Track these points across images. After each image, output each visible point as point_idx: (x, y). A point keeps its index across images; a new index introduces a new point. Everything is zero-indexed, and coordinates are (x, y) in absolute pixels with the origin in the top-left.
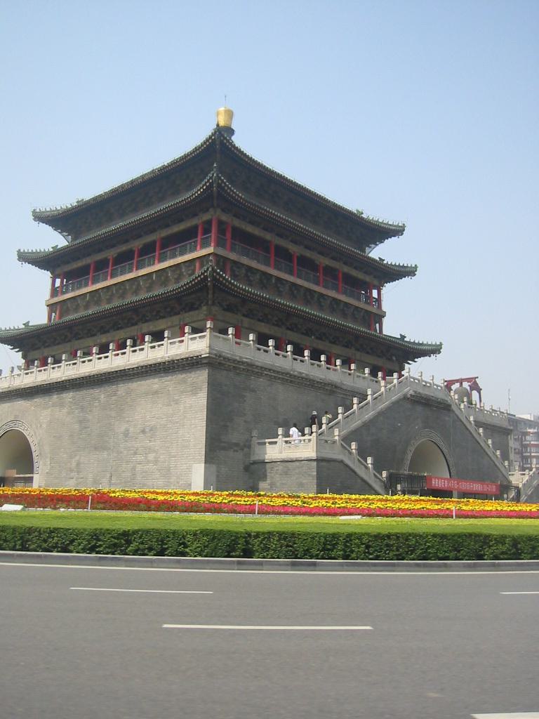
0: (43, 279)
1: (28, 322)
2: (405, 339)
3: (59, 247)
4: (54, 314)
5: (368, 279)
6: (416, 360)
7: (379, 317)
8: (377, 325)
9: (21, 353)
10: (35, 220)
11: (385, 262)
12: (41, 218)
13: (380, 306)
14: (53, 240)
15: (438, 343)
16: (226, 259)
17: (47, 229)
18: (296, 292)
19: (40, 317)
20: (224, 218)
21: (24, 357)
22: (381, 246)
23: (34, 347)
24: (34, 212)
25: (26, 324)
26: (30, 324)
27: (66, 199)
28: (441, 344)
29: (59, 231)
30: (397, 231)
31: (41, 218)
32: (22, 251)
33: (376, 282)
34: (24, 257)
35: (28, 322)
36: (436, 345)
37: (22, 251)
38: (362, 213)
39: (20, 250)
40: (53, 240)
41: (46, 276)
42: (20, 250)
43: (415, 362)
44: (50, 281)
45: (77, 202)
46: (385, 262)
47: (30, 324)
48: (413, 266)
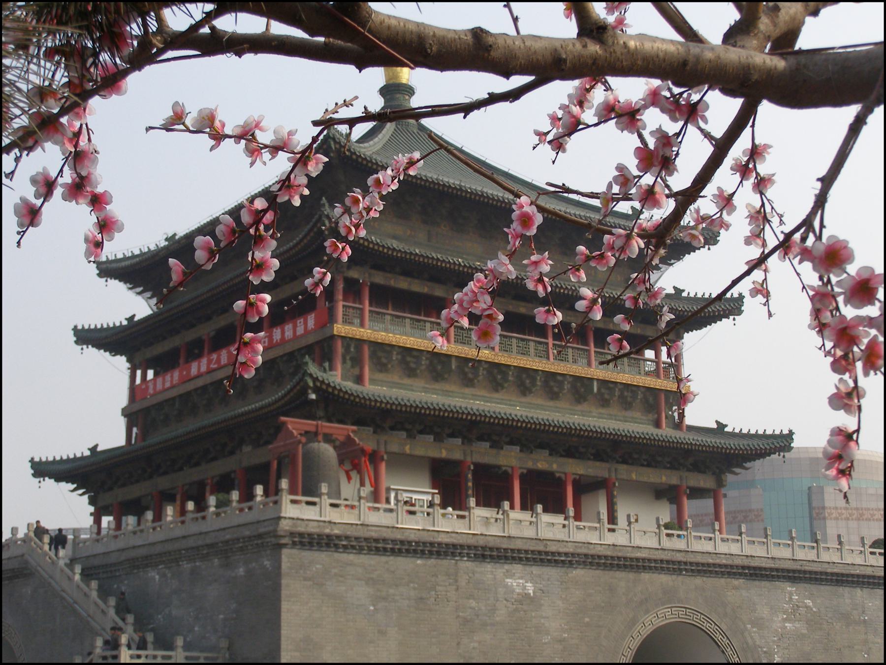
0: (117, 368)
1: (97, 446)
2: (726, 430)
3: (136, 319)
4: (135, 430)
9: (86, 496)
11: (684, 294)
14: (129, 305)
15: (786, 432)
16: (360, 342)
17: (117, 287)
18: (499, 377)
19: (113, 435)
21: (92, 502)
25: (93, 450)
26: (99, 449)
28: (791, 433)
29: (140, 289)
32: (80, 327)
34: (87, 337)
35: (97, 446)
36: (781, 436)
37: (80, 327)
39: (76, 327)
40: (129, 305)
41: (121, 362)
42: (76, 327)
43: (747, 469)
45: (166, 239)
46: (684, 294)
47: (99, 449)
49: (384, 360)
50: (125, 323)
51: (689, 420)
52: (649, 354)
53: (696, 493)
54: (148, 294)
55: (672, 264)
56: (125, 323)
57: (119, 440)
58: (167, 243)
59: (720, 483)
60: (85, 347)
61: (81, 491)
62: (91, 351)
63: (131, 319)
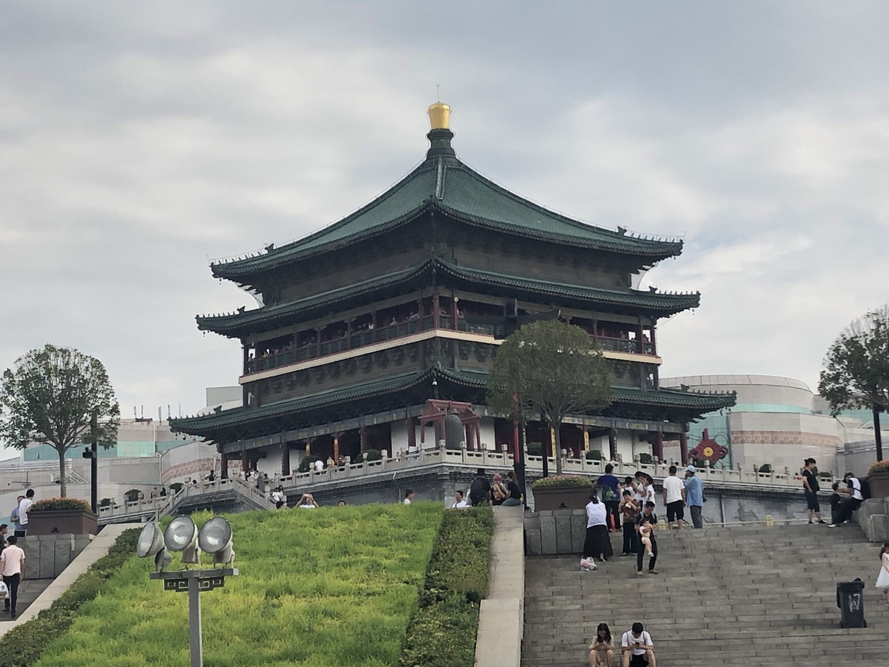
0: (233, 349)
4: (250, 394)
5: (633, 321)
6: (703, 415)
7: (654, 368)
8: (651, 376)
10: (214, 276)
11: (657, 292)
12: (221, 271)
13: (654, 353)
20: (446, 294)
22: (652, 270)
23: (233, 438)
24: (212, 266)
27: (249, 246)
29: (248, 287)
30: (673, 249)
31: (221, 271)
33: (645, 321)
38: (625, 231)
44: (242, 352)
46: (657, 292)
48: (695, 293)
49: (465, 352)
50: (237, 313)
51: (662, 385)
52: (632, 335)
53: (669, 436)
54: (254, 291)
55: (647, 270)
56: (237, 313)
57: (239, 403)
58: (266, 252)
59: (686, 429)
60: (206, 331)
61: (210, 442)
62: (212, 336)
63: (241, 310)
